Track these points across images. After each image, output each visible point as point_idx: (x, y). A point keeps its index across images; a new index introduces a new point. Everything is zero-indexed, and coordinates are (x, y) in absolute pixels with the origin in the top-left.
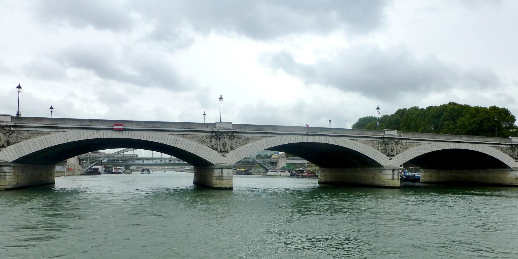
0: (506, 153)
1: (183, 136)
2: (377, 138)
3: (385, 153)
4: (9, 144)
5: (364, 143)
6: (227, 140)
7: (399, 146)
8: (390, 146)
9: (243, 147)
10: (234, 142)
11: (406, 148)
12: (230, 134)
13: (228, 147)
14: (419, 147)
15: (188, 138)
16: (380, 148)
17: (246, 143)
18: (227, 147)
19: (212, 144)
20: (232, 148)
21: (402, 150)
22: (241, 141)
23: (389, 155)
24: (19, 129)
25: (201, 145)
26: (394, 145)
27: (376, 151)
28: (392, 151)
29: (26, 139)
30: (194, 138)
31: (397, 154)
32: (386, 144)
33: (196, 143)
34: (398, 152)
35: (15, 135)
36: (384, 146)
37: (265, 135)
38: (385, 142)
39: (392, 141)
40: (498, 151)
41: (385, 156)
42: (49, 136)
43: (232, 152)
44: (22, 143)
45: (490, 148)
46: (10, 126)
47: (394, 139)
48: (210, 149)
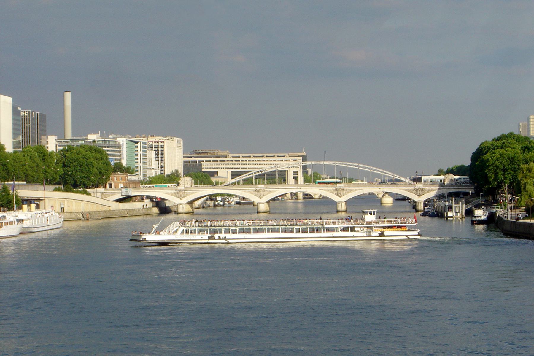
0: (412, 193)
1: (244, 191)
2: (332, 188)
3: (337, 195)
4: (184, 197)
5: (326, 191)
6: (262, 193)
7: (344, 192)
8: (339, 192)
9: (269, 195)
10: (264, 193)
11: (349, 192)
12: (263, 190)
13: (262, 195)
14: (356, 191)
15: (246, 192)
16: (334, 193)
17: (270, 193)
18: (262, 195)
19: (256, 194)
20: (264, 195)
21: (347, 193)
22: (268, 192)
23: (339, 196)
24: (187, 191)
25: (251, 195)
26: (341, 191)
27: (333, 194)
28: (340, 194)
29: (189, 195)
30: (248, 192)
31: (343, 195)
32: (337, 191)
33: (249, 194)
34: (344, 194)
35: (186, 194)
36: (336, 192)
37: (278, 189)
38: (337, 190)
39: (340, 189)
40: (407, 192)
41: (337, 196)
42: (195, 194)
43: (264, 197)
44: (188, 196)
45: (401, 190)
46: (184, 191)
47: (341, 188)
48: (255, 196)
